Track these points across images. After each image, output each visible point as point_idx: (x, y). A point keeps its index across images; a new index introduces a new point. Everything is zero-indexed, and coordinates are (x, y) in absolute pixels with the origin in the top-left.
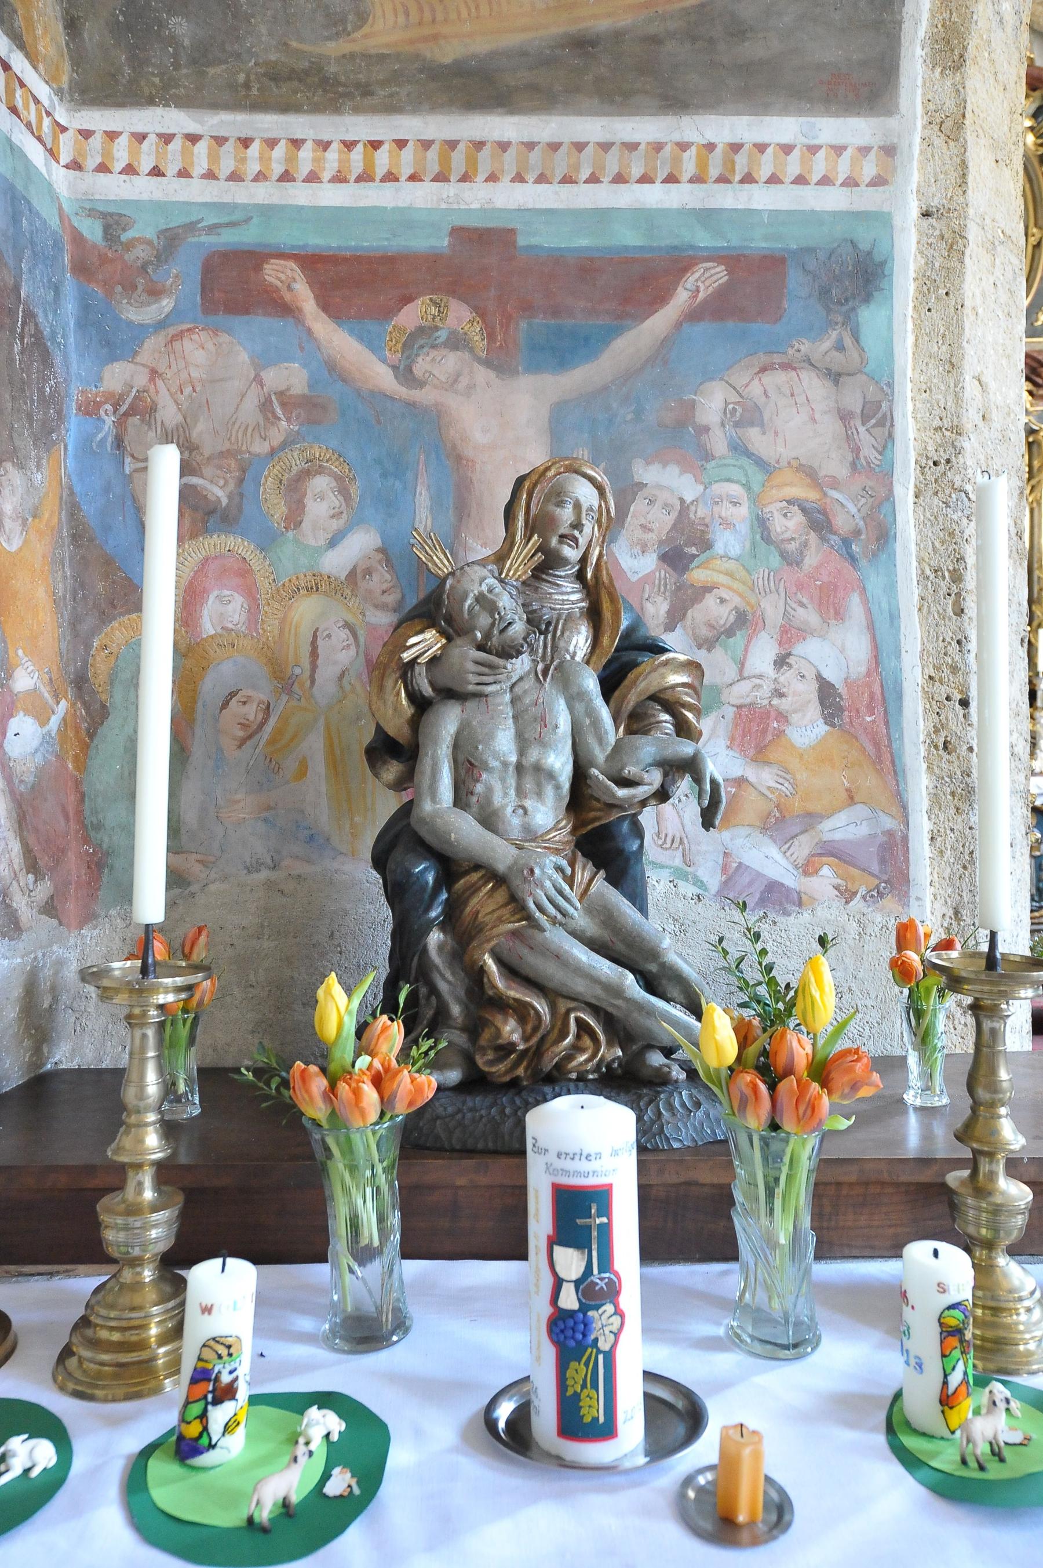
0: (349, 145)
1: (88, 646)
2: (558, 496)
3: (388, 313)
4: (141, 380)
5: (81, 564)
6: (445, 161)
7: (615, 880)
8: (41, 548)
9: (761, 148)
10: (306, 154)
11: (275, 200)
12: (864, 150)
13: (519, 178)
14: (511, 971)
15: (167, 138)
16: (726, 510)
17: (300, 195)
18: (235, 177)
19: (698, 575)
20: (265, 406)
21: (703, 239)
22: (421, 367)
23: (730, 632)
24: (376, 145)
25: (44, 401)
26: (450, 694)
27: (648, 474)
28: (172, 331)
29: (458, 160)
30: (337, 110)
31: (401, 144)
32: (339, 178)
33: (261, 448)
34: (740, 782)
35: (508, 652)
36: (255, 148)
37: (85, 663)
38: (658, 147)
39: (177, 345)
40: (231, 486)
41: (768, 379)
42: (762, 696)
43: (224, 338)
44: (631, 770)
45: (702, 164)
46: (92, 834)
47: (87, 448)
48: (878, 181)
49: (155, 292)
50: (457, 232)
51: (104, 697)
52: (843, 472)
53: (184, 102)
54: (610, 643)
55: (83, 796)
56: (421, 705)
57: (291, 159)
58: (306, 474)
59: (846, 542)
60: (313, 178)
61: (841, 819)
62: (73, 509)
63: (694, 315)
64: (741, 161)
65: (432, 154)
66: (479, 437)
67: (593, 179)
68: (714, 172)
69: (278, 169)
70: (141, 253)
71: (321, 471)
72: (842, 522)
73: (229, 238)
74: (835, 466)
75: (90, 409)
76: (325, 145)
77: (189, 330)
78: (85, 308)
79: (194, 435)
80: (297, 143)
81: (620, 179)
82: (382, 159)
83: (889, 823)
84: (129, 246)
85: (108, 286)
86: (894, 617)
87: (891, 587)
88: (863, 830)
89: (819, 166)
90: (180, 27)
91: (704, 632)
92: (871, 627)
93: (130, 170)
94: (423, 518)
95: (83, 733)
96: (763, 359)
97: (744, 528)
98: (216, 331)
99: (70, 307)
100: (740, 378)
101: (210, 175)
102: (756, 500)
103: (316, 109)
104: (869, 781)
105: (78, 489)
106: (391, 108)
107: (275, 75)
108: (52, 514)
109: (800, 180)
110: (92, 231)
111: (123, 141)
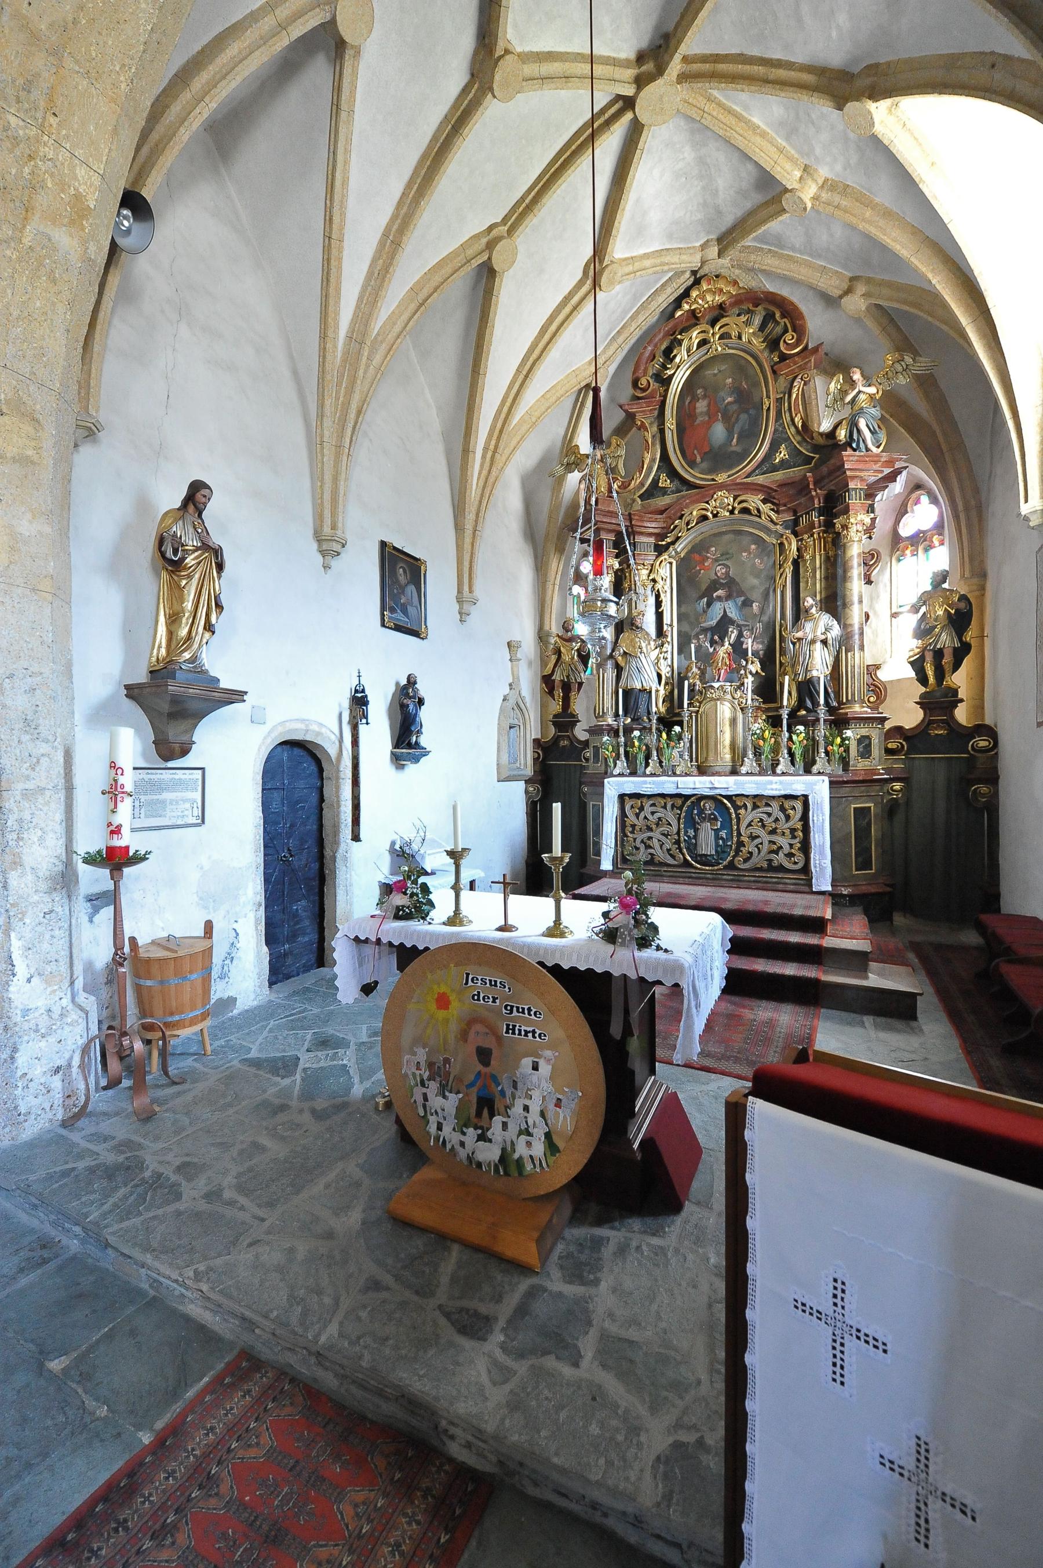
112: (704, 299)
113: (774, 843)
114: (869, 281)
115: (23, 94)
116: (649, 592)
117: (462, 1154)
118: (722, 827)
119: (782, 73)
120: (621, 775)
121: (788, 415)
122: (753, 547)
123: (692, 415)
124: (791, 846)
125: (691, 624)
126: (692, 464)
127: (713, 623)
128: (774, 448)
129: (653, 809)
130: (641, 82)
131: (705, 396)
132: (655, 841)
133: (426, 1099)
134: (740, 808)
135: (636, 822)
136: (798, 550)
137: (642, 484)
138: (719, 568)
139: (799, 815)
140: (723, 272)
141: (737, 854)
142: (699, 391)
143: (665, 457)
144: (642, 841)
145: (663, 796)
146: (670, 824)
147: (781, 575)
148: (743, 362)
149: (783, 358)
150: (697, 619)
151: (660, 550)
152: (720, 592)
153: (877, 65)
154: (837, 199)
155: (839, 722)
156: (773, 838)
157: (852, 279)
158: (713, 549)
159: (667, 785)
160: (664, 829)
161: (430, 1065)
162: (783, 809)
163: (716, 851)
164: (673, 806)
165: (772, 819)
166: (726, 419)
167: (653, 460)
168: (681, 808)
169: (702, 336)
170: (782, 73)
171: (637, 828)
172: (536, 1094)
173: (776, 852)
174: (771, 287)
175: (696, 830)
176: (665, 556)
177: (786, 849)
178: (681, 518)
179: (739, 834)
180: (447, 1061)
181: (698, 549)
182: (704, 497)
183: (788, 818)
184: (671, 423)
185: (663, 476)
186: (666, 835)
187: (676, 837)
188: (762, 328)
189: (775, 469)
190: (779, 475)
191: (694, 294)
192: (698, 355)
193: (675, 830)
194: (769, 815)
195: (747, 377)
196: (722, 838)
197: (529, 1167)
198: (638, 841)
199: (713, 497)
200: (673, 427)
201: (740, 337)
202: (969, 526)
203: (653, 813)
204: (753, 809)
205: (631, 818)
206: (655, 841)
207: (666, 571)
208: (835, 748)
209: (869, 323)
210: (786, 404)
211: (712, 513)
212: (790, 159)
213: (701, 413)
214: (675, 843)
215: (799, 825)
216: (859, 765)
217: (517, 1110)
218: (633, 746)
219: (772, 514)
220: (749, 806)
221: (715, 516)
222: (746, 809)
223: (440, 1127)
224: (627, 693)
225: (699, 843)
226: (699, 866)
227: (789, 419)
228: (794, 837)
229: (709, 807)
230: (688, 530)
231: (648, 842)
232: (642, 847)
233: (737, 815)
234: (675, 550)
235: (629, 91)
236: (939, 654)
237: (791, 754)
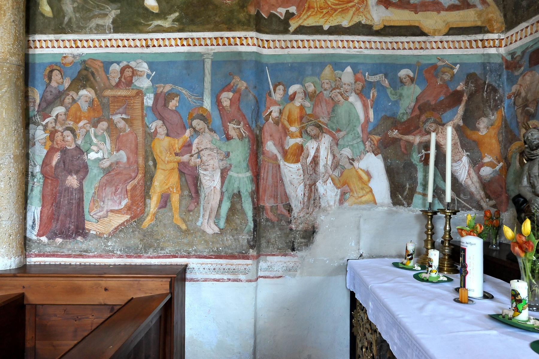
1: (507, 150)
4: (518, 88)
5: (506, 132)
8: (493, 132)
25: (495, 100)
28: (523, 74)
37: (507, 154)
39: (524, 77)
40: (535, 108)
43: (534, 72)
46: (507, 192)
47: (509, 106)
49: (520, 67)
51: (510, 161)
53: (525, 20)
55: (506, 183)
70: (518, 59)
75: (509, 97)
77: (527, 73)
78: (508, 75)
79: (528, 97)
95: (506, 170)
99: (505, 77)
105: (507, 116)
108: (498, 123)
110: (509, 58)
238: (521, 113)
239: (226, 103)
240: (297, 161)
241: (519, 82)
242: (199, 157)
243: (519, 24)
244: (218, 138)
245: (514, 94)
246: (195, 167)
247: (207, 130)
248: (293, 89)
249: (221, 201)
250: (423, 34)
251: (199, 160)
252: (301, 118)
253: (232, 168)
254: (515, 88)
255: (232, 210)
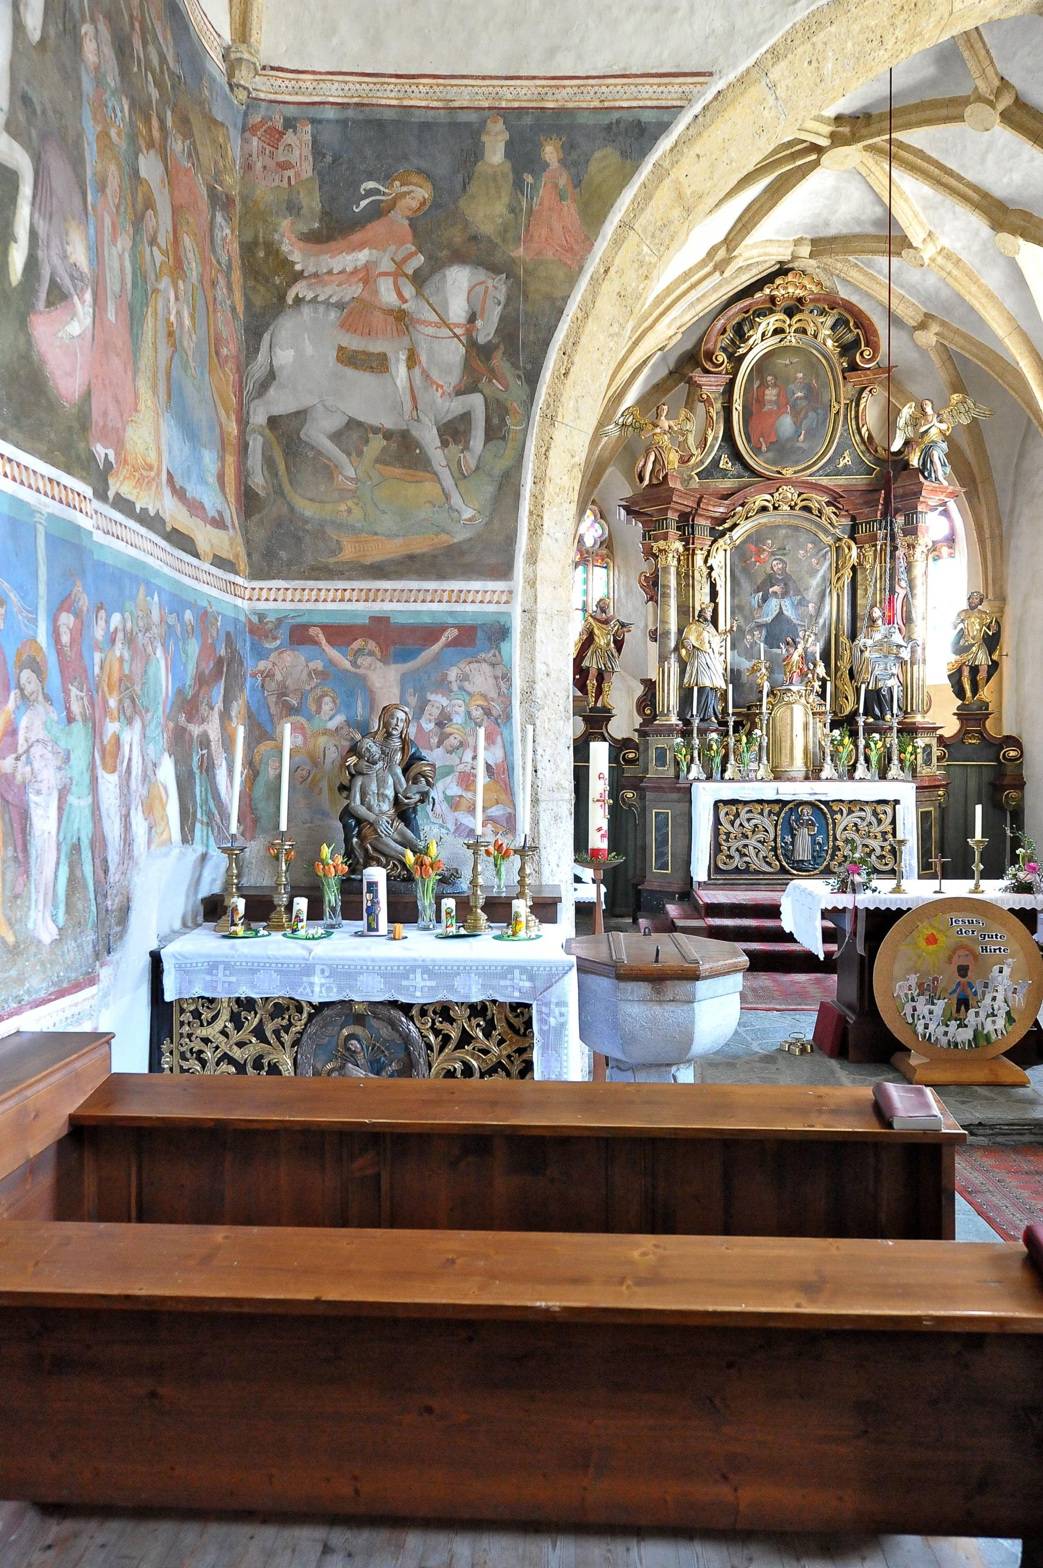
0: (337, 590)
2: (392, 716)
3: (349, 644)
4: (270, 666)
6: (367, 595)
7: (407, 825)
9: (469, 591)
10: (323, 593)
11: (313, 608)
12: (502, 592)
13: (391, 601)
14: (375, 849)
15: (279, 589)
16: (457, 709)
17: (321, 606)
18: (300, 601)
19: (448, 730)
20: (309, 675)
21: (450, 621)
22: (358, 662)
23: (458, 749)
24: (345, 590)
26: (361, 774)
27: (431, 697)
29: (371, 595)
30: (333, 579)
31: (353, 590)
32: (333, 601)
33: (308, 688)
34: (461, 796)
35: (375, 763)
36: (306, 591)
38: (436, 591)
41: (472, 666)
42: (468, 769)
44: (409, 795)
45: (450, 596)
47: (253, 688)
48: (507, 602)
49: (275, 638)
50: (370, 617)
52: (495, 696)
54: (407, 759)
56: (352, 776)
57: (318, 595)
58: (322, 696)
59: (496, 719)
60: (325, 600)
61: (494, 809)
62: (249, 708)
63: (448, 645)
64: (462, 595)
65: (363, 593)
66: (378, 685)
67: (415, 601)
68: (454, 599)
69: (314, 598)
70: (270, 626)
71: (327, 695)
72: (495, 713)
73: (299, 620)
74: (493, 694)
75: (254, 676)
76: (329, 590)
78: (252, 644)
80: (320, 590)
81: (423, 601)
82: (347, 595)
83: (509, 810)
84: (266, 624)
85: (260, 637)
86: (512, 743)
87: (511, 733)
88: (501, 812)
89: (488, 597)
90: (283, 554)
91: (449, 748)
92: (504, 747)
93: (267, 600)
94: (360, 711)
96: (469, 659)
97: (463, 714)
98: (293, 650)
100: (462, 665)
101: (292, 600)
102: (467, 705)
103: (326, 579)
104: (503, 797)
106: (350, 579)
107: (313, 569)
109: (481, 602)
110: (255, 619)
111: (265, 591)
112: (785, 290)
113: (867, 846)
114: (943, 324)
115: (658, 233)
116: (704, 580)
117: (944, 1041)
118: (819, 833)
119: (953, 182)
120: (698, 780)
121: (854, 422)
122: (810, 545)
123: (761, 401)
124: (882, 848)
125: (745, 618)
126: (757, 451)
127: (769, 619)
128: (839, 454)
129: (750, 815)
130: (837, 140)
131: (775, 385)
132: (751, 848)
133: (915, 1009)
134: (836, 813)
135: (731, 829)
136: (859, 557)
137: (702, 462)
138: (775, 562)
139: (889, 820)
140: (809, 271)
141: (832, 859)
142: (769, 378)
143: (729, 436)
144: (737, 850)
145: (760, 802)
146: (766, 831)
147: (839, 578)
148: (814, 360)
149: (853, 367)
150: (752, 613)
151: (717, 536)
152: (776, 588)
153: (1031, 215)
154: (950, 267)
155: (908, 731)
156: (867, 841)
157: (927, 316)
158: (770, 542)
159: (768, 791)
160: (761, 836)
161: (920, 986)
162: (875, 813)
163: (813, 856)
164: (770, 812)
165: (865, 823)
166: (796, 414)
167: (715, 438)
168: (778, 815)
169: (778, 325)
170: (953, 182)
171: (732, 836)
172: (1000, 988)
173: (869, 855)
174: (854, 299)
175: (793, 836)
176: (721, 541)
177: (878, 852)
178: (743, 505)
179: (835, 839)
180: (935, 979)
181: (756, 538)
182: (770, 487)
183: (880, 821)
184: (738, 405)
185: (724, 458)
186: (762, 842)
187: (773, 844)
188: (833, 328)
189: (838, 473)
190: (842, 480)
191: (778, 281)
192: (772, 342)
193: (772, 837)
194: (863, 819)
195: (817, 376)
196: (819, 843)
197: (994, 1037)
198: (733, 849)
199: (778, 490)
200: (740, 408)
201: (815, 336)
202: (993, 553)
203: (749, 820)
204: (848, 814)
205: (726, 827)
206: (751, 848)
207: (719, 559)
208: (908, 756)
209: (933, 356)
210: (853, 412)
211: (773, 505)
212: (921, 224)
213: (770, 401)
214: (771, 850)
215: (889, 828)
216: (924, 771)
217: (988, 1000)
218: (710, 748)
219: (833, 516)
220: (845, 812)
221: (775, 508)
222: (842, 814)
223: (926, 1027)
224: (702, 690)
225: (797, 848)
226: (795, 872)
227: (854, 427)
228: (885, 840)
229: (807, 810)
230: (747, 518)
231: (745, 851)
232: (737, 855)
233: (834, 820)
234: (731, 538)
235: (824, 142)
236: (974, 670)
237: (867, 760)
238: (276, 703)
239: (65, 639)
240: (113, 771)
241: (271, 658)
242: (29, 762)
243: (274, 578)
244: (56, 718)
245: (262, 673)
246: (24, 787)
247: (41, 698)
248: (116, 619)
249: (58, 864)
250: (197, 556)
251: (28, 769)
252: (120, 680)
253: (74, 788)
254: (262, 665)
255: (74, 883)
